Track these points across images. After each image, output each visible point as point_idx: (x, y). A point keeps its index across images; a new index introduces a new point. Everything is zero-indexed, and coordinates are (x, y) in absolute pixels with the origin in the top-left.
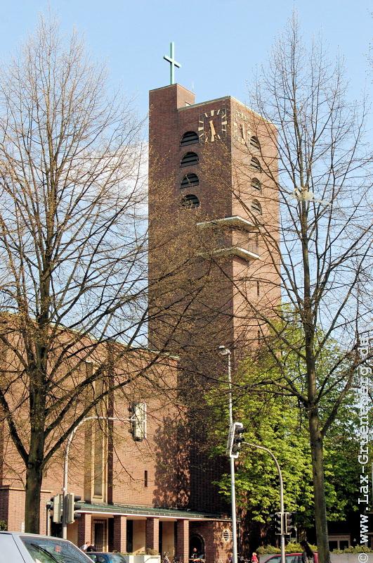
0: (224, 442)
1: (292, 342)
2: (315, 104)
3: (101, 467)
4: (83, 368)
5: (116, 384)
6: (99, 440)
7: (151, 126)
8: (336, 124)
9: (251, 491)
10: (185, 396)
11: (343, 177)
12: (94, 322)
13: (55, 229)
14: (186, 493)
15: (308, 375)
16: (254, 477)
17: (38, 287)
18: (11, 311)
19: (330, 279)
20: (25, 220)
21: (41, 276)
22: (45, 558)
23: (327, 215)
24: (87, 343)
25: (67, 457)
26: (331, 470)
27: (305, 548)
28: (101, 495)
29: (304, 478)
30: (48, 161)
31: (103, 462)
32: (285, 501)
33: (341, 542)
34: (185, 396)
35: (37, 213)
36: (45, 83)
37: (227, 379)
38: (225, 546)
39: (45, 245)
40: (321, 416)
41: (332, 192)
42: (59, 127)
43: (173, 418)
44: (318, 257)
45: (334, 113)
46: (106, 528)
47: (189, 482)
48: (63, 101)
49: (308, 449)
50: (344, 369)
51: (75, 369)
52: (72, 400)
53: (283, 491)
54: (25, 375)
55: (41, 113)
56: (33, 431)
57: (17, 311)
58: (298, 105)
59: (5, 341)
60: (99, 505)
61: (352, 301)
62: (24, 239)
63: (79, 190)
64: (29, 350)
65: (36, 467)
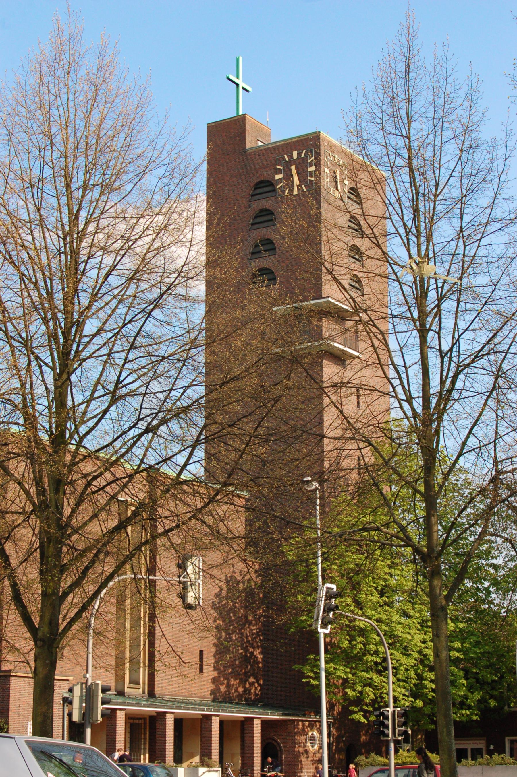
0: (310, 611)
1: (405, 472)
2: (438, 143)
3: (139, 645)
4: (114, 508)
5: (160, 530)
6: (136, 608)
7: (210, 173)
8: (467, 171)
9: (348, 678)
10: (256, 546)
11: (476, 244)
12: (129, 444)
13: (76, 316)
14: (258, 681)
15: (428, 519)
16: (351, 659)
17: (52, 395)
18: (14, 429)
19: (459, 385)
20: (34, 303)
21: (55, 380)
22: (60, 771)
23: (455, 297)
24: (119, 474)
25: (91, 631)
26: (458, 650)
27: (423, 758)
28: (139, 683)
29: (422, 662)
30: (66, 220)
31: (142, 638)
32: (394, 693)
33: (472, 750)
34: (256, 546)
35: (50, 294)
36: (62, 112)
37: (315, 523)
38: (311, 754)
39: (61, 337)
40: (445, 575)
41: (461, 264)
42: (81, 174)
43: (239, 578)
44: (441, 355)
45: (464, 155)
46: (145, 730)
47: (260, 665)
48: (87, 138)
49: (427, 621)
50: (478, 510)
51: (103, 509)
52: (99, 552)
53: (392, 679)
54: (34, 517)
55: (56, 154)
56: (44, 594)
57: (22, 429)
58: (415, 145)
59: (6, 471)
60: (136, 697)
61: (489, 416)
62: (33, 328)
63: (108, 260)
64: (38, 482)
65: (48, 646)
